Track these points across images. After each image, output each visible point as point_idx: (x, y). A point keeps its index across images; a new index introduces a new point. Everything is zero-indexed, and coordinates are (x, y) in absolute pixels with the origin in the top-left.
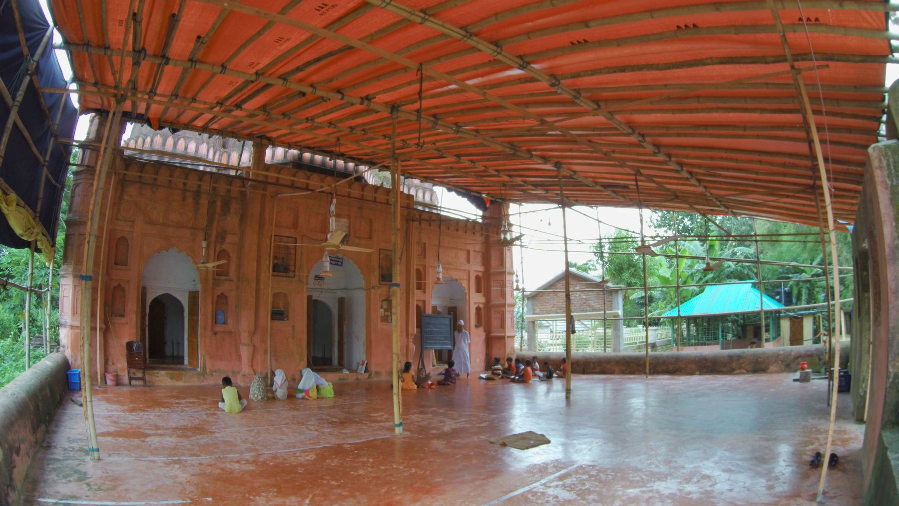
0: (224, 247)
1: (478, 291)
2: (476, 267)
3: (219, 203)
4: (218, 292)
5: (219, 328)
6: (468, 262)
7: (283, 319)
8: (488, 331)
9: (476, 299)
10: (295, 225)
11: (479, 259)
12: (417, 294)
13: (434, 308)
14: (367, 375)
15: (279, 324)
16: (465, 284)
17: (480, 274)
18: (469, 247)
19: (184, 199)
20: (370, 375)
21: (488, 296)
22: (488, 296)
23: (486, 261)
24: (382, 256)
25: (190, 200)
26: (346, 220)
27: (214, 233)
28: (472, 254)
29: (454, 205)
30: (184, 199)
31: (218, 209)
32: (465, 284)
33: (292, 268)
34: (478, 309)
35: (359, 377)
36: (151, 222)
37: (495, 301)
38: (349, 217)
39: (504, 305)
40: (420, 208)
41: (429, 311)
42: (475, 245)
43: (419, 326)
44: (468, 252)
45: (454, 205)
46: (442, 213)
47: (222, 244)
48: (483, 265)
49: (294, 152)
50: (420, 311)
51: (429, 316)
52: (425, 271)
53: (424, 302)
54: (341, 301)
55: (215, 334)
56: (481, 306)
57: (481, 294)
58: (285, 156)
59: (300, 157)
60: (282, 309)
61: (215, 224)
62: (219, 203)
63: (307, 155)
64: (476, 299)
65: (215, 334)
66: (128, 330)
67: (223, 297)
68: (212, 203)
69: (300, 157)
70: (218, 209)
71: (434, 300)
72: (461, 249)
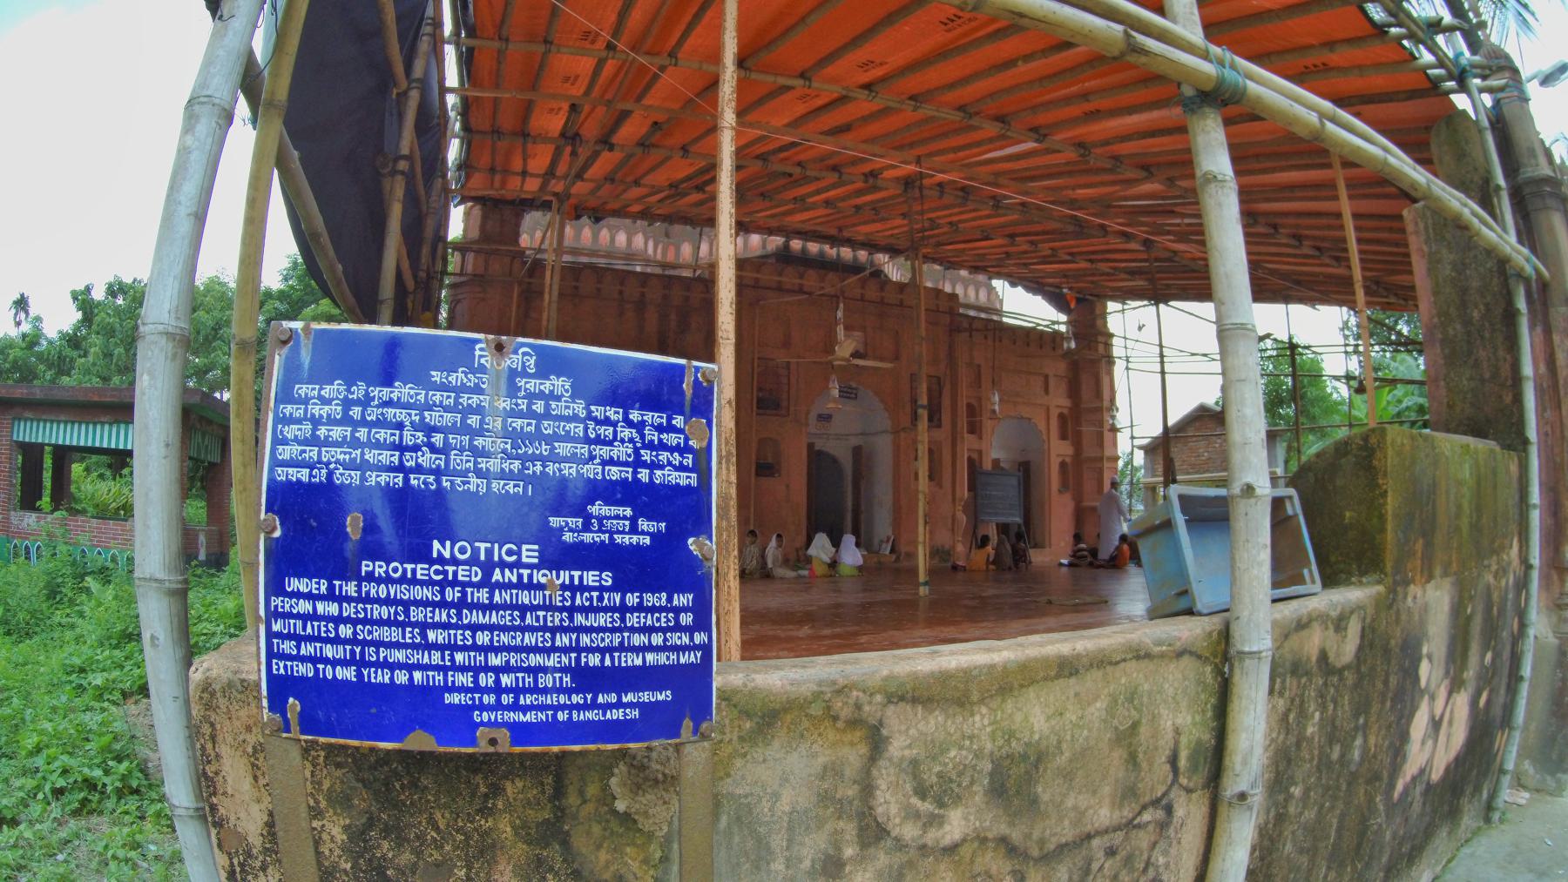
1: (1063, 437)
2: (1059, 401)
3: (673, 317)
6: (1047, 391)
7: (772, 475)
8: (1078, 500)
9: (1060, 450)
10: (786, 344)
11: (1063, 388)
12: (969, 441)
13: (996, 462)
15: (767, 482)
16: (1042, 426)
17: (1066, 411)
21: (1078, 445)
22: (1078, 445)
23: (1074, 392)
28: (1052, 381)
29: (1024, 307)
32: (1042, 426)
33: (784, 404)
34: (1063, 465)
37: (1089, 451)
38: (863, 329)
39: (1101, 459)
40: (972, 313)
41: (987, 465)
42: (1057, 368)
43: (972, 488)
44: (1046, 377)
45: (1024, 307)
46: (1005, 320)
48: (1070, 396)
49: (777, 241)
50: (974, 467)
51: (988, 474)
53: (980, 452)
54: (857, 452)
56: (1068, 460)
58: (764, 247)
59: (786, 246)
60: (770, 460)
62: (673, 317)
63: (796, 244)
64: (1060, 450)
69: (786, 246)
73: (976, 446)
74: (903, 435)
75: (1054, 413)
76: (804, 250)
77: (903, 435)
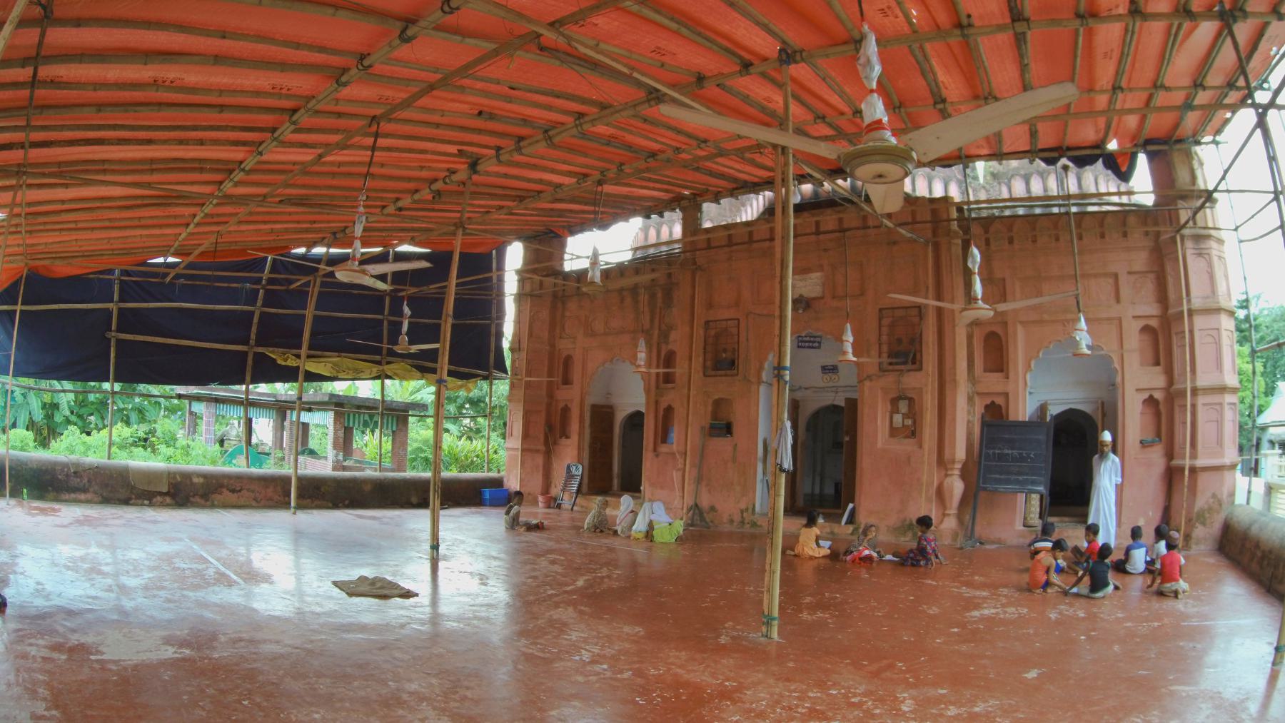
0: (670, 347)
4: (663, 405)
5: (663, 449)
6: (1118, 301)
14: (851, 528)
18: (1112, 268)
19: (622, 300)
20: (856, 529)
24: (885, 322)
25: (628, 300)
26: (818, 274)
27: (656, 332)
28: (1123, 279)
30: (622, 300)
35: (836, 530)
36: (593, 334)
38: (820, 268)
44: (1116, 276)
47: (667, 343)
52: (1006, 334)
53: (1006, 395)
55: (657, 456)
57: (1158, 369)
62: (659, 295)
65: (657, 456)
68: (653, 296)
71: (1040, 392)
72: (1096, 276)
73: (999, 389)
74: (867, 383)
77: (867, 383)
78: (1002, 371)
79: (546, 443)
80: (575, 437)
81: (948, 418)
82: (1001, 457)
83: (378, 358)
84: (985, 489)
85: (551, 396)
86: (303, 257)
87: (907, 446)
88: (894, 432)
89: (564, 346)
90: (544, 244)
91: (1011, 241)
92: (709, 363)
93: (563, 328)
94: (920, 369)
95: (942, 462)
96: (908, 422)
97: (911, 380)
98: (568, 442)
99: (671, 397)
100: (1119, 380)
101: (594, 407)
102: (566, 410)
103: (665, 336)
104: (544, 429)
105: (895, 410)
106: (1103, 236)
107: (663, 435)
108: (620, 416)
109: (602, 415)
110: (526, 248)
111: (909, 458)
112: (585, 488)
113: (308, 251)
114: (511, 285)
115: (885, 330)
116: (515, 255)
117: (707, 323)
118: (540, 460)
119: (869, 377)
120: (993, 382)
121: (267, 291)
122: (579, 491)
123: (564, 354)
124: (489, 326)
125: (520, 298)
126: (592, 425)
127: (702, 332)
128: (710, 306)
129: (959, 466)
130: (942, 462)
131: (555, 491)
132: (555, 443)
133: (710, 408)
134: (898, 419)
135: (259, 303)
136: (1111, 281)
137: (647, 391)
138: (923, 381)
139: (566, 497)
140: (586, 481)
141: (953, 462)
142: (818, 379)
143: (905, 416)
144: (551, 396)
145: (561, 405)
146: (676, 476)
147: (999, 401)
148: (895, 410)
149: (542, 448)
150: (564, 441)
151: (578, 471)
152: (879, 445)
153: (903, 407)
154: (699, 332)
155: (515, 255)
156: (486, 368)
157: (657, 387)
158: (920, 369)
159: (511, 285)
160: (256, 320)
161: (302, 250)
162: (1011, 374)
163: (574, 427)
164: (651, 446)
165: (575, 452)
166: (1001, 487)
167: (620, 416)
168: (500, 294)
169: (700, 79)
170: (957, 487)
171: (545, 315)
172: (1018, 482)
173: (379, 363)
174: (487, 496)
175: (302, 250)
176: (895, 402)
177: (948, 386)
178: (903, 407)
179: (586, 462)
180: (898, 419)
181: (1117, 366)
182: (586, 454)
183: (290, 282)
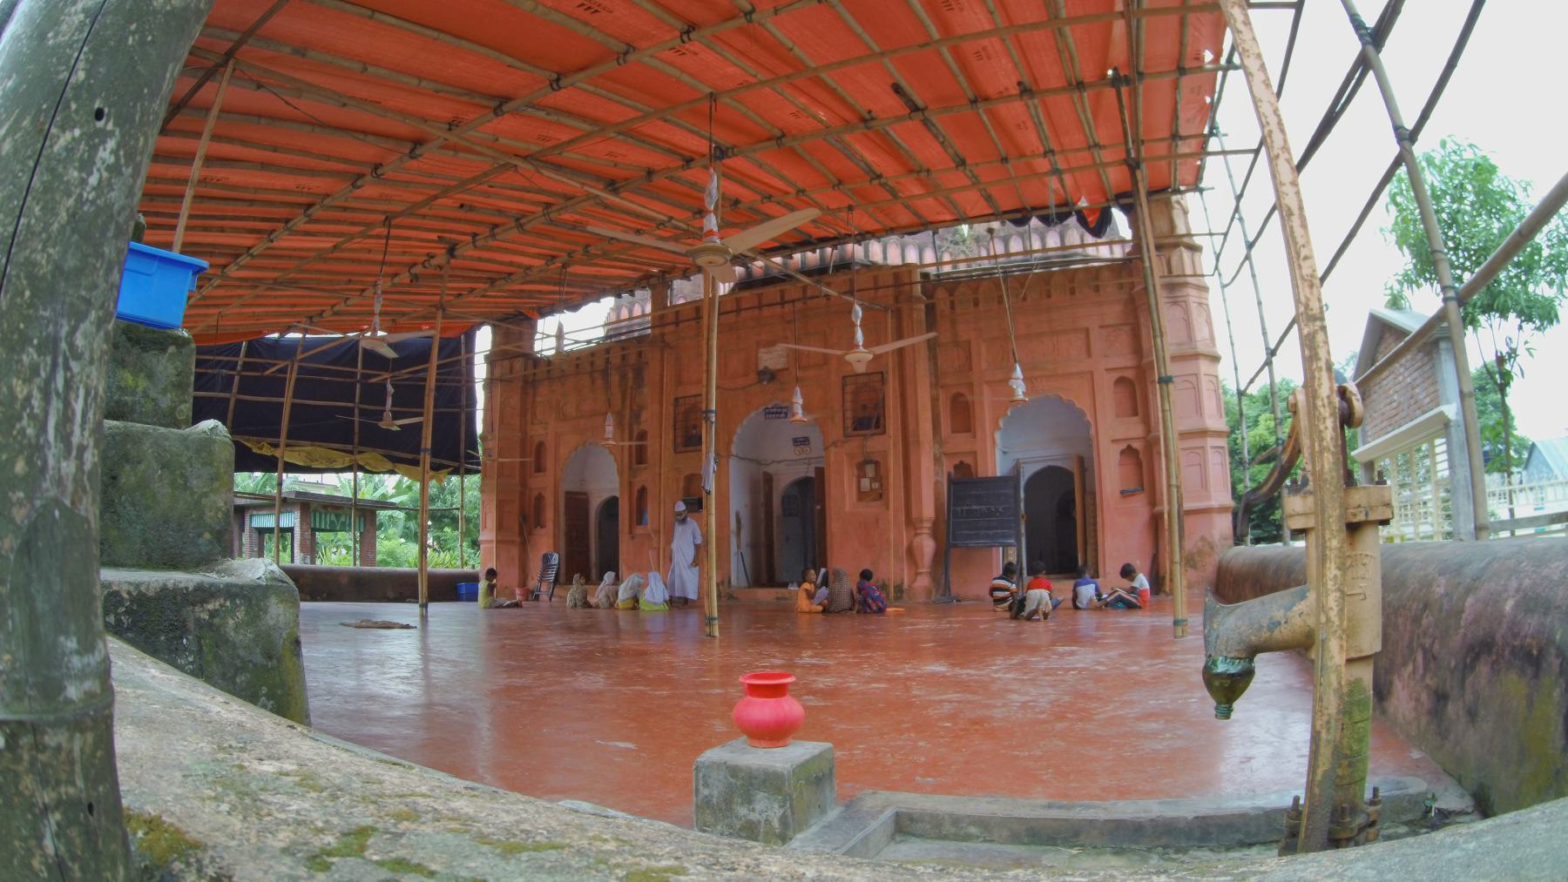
2: (1115, 358)
3: (630, 375)
4: (637, 487)
5: (639, 530)
6: (1089, 354)
17: (1130, 374)
19: (593, 383)
24: (849, 389)
25: (599, 382)
27: (627, 412)
30: (593, 383)
31: (630, 383)
32: (1083, 403)
34: (1129, 452)
44: (1087, 330)
53: (974, 453)
56: (1136, 445)
59: (749, 272)
61: (628, 403)
62: (630, 375)
66: (547, 544)
67: (643, 491)
68: (623, 377)
69: (749, 272)
70: (630, 383)
71: (1008, 452)
74: (833, 449)
75: (1105, 383)
76: (766, 268)
77: (833, 449)
78: (968, 430)
79: (521, 533)
80: (550, 526)
81: (913, 479)
82: (970, 513)
83: (349, 447)
84: (955, 546)
85: (524, 483)
86: (276, 341)
87: (871, 509)
88: (862, 496)
89: (537, 432)
90: (515, 326)
91: (976, 304)
92: (679, 440)
93: (534, 414)
94: (884, 432)
95: (911, 522)
96: (876, 485)
97: (875, 444)
98: (544, 531)
99: (644, 477)
100: (1092, 432)
101: (568, 493)
102: (540, 498)
103: (636, 416)
104: (519, 517)
105: (861, 475)
106: (1073, 292)
107: (639, 516)
108: (596, 503)
109: (576, 503)
110: (494, 333)
111: (877, 521)
112: (562, 578)
113: (282, 335)
114: (480, 371)
115: (848, 397)
116: (484, 339)
117: (677, 399)
118: (515, 552)
119: (834, 444)
120: (960, 443)
121: (242, 378)
122: (556, 581)
123: (537, 440)
124: (459, 414)
125: (490, 383)
126: (567, 513)
127: (671, 408)
128: (679, 382)
129: (928, 525)
130: (911, 522)
131: (533, 583)
132: (530, 534)
133: (682, 484)
134: (865, 483)
135: (235, 389)
136: (1082, 336)
137: (621, 473)
138: (887, 444)
139: (544, 588)
140: (563, 571)
141: (922, 521)
142: (789, 452)
143: (872, 480)
144: (524, 483)
145: (535, 493)
146: (651, 554)
147: (968, 460)
148: (861, 475)
149: (517, 539)
150: (539, 531)
151: (555, 559)
152: (847, 509)
153: (870, 470)
154: (668, 409)
155: (484, 339)
156: (456, 458)
157: (630, 468)
158: (884, 432)
159: (480, 371)
160: (231, 407)
161: (276, 335)
162: (979, 434)
163: (549, 514)
164: (626, 528)
165: (551, 541)
166: (972, 543)
167: (596, 503)
168: (470, 380)
169: (650, 173)
170: (927, 546)
171: (515, 400)
172: (988, 536)
173: (351, 452)
174: (463, 591)
175: (276, 335)
176: (861, 467)
177: (912, 447)
178: (870, 470)
179: (563, 552)
180: (865, 483)
181: (1089, 418)
182: (562, 543)
183: (265, 367)
